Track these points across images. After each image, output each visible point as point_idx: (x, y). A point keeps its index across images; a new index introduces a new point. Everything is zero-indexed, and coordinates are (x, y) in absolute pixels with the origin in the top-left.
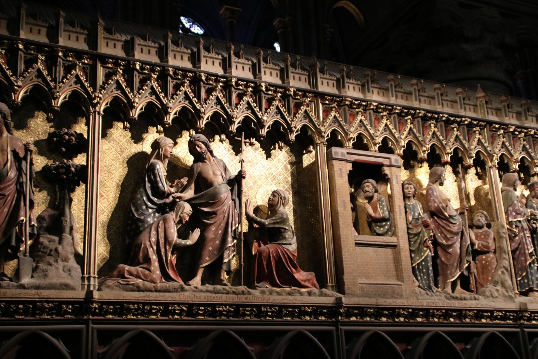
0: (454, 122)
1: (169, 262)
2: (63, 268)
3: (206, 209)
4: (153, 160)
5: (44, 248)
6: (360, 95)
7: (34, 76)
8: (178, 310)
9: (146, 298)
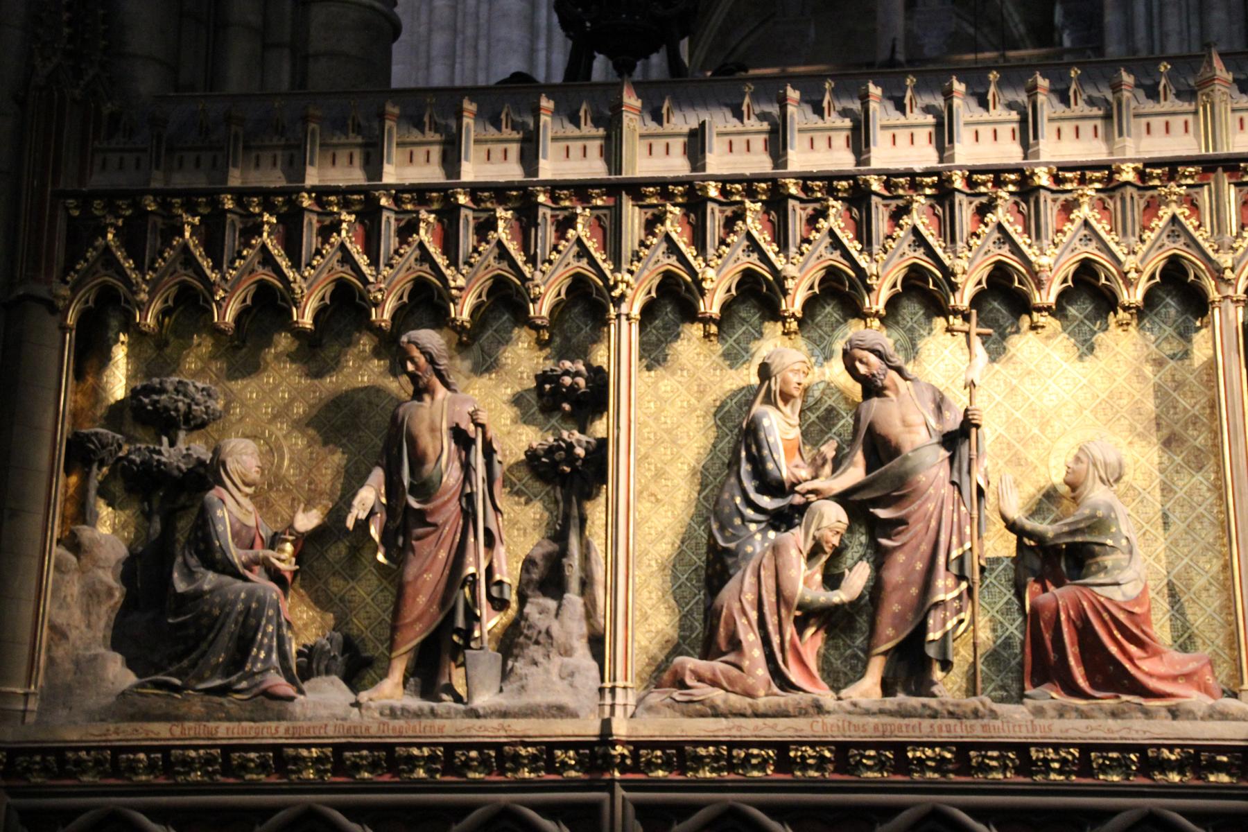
1: (787, 645)
2: (560, 670)
3: (882, 513)
4: (758, 408)
5: (530, 627)
7: (491, 259)
8: (811, 757)
9: (734, 732)
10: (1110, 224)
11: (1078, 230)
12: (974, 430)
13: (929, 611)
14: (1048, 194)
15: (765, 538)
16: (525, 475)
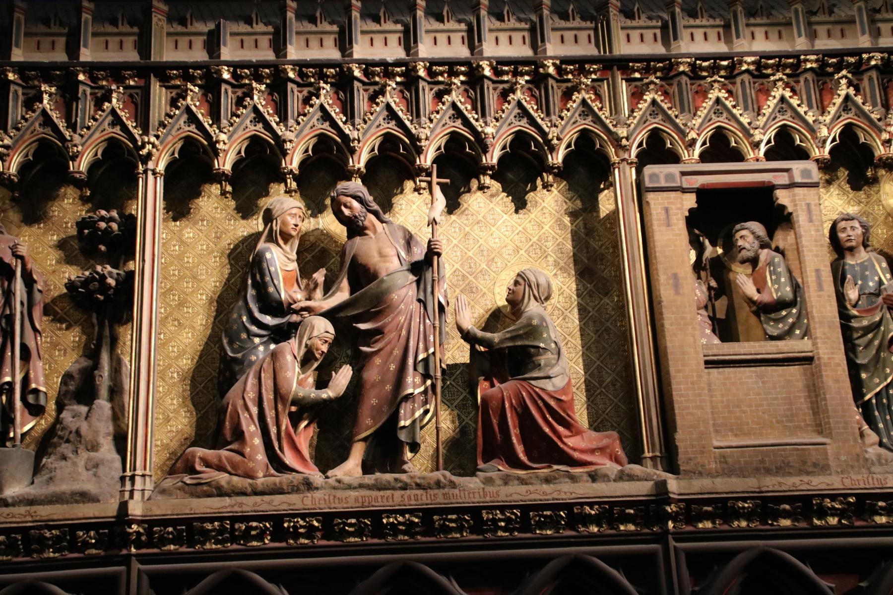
1: (283, 434)
3: (363, 326)
4: (261, 245)
5: (63, 429)
6: (721, 48)
7: (37, 125)
8: (302, 527)
9: (236, 509)
10: (537, 104)
11: (513, 109)
12: (436, 257)
13: (400, 403)
14: (490, 83)
15: (267, 348)
16: (67, 305)
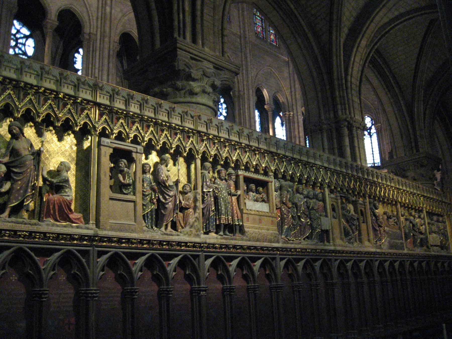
0: (179, 129)
